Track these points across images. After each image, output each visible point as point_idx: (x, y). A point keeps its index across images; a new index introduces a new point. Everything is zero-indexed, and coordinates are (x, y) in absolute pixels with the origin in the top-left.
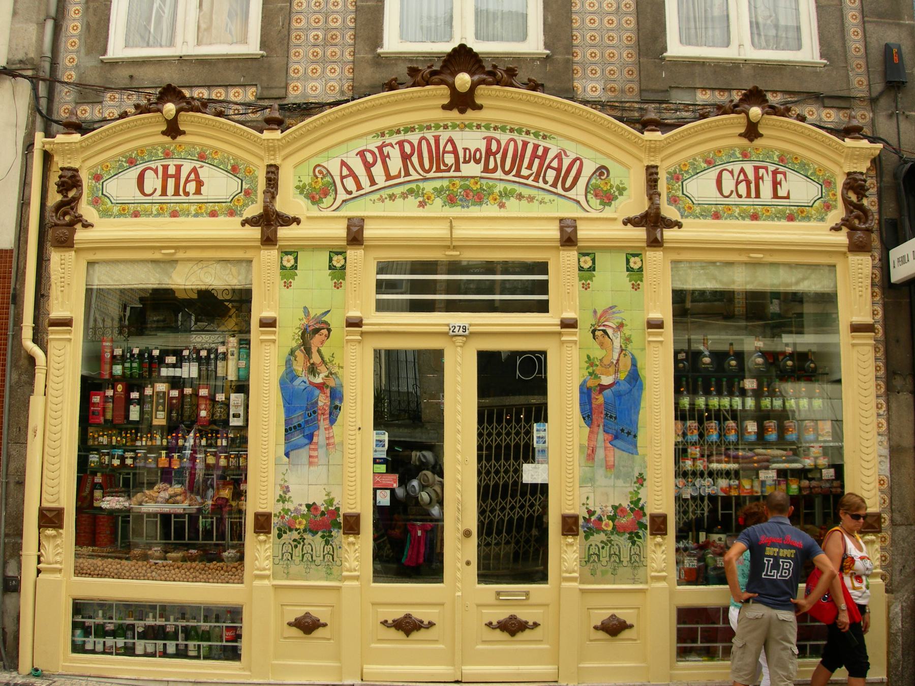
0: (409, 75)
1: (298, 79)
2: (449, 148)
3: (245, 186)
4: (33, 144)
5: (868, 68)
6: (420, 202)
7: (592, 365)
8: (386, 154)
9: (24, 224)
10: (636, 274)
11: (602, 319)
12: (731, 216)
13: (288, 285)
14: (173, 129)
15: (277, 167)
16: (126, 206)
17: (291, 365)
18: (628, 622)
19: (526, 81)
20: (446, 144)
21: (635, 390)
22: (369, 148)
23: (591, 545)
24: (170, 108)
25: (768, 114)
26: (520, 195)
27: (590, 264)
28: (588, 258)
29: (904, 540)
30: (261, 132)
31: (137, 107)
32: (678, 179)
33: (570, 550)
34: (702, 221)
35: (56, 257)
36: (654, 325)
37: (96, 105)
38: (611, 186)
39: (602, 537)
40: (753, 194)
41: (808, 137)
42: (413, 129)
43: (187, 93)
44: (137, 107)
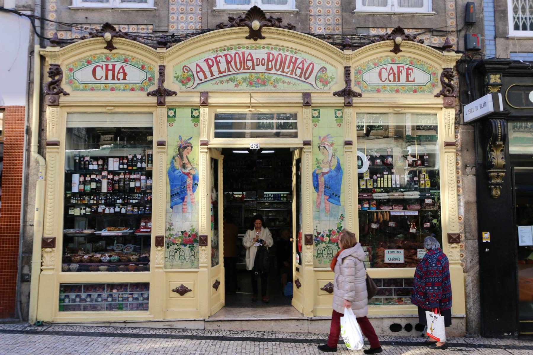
0: (229, 21)
1: (174, 22)
2: (249, 58)
3: (149, 76)
6: (235, 85)
8: (218, 61)
10: (339, 119)
11: (323, 142)
13: (171, 125)
15: (164, 66)
19: (286, 24)
20: (248, 56)
21: (339, 175)
22: (210, 58)
24: (108, 35)
25: (405, 40)
26: (284, 81)
27: (317, 114)
30: (156, 49)
32: (360, 73)
33: (308, 251)
36: (348, 143)
37: (68, 32)
38: (328, 77)
39: (324, 245)
40: (397, 80)
41: (425, 51)
42: (231, 49)
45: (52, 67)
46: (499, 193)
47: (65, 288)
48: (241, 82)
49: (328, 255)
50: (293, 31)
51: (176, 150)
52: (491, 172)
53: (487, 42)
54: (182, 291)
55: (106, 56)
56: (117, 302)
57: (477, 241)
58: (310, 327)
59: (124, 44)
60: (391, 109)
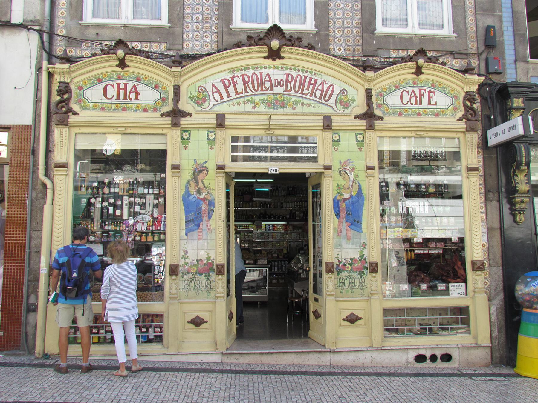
0: (247, 40)
1: (189, 40)
2: (267, 79)
4: (42, 68)
7: (339, 188)
8: (235, 81)
9: (38, 112)
10: (361, 144)
13: (186, 148)
16: (97, 104)
17: (188, 189)
20: (266, 76)
23: (340, 278)
24: (120, 53)
25: (427, 62)
26: (303, 103)
27: (338, 138)
30: (171, 68)
32: (381, 95)
35: (57, 132)
36: (370, 168)
40: (418, 103)
41: (447, 74)
42: (249, 69)
43: (129, 44)
44: (102, 50)
45: (62, 84)
48: (259, 104)
50: (313, 51)
51: (191, 174)
53: (507, 66)
54: (197, 322)
55: (117, 74)
57: (501, 268)
58: (332, 359)
59: (137, 62)
60: (413, 132)
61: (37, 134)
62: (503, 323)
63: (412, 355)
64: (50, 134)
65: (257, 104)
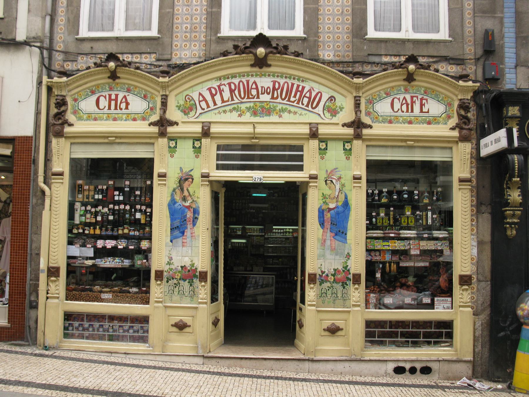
0: (234, 48)
2: (254, 86)
5: (475, 42)
6: (239, 114)
7: (325, 198)
8: (222, 89)
9: (38, 123)
10: (348, 152)
12: (398, 122)
13: (172, 156)
14: (113, 76)
16: (90, 115)
18: (341, 327)
19: (293, 51)
22: (214, 86)
25: (418, 68)
26: (290, 111)
27: (325, 146)
28: (324, 144)
29: (484, 290)
31: (95, 64)
34: (383, 124)
35: (54, 141)
36: (357, 178)
39: (328, 284)
40: (410, 111)
42: (235, 77)
44: (95, 64)
45: (59, 97)
46: (514, 232)
47: (69, 316)
49: (332, 294)
52: (507, 210)
54: (181, 326)
56: (118, 333)
57: (489, 283)
61: (37, 144)
62: (487, 339)
63: (391, 366)
64: (49, 144)
65: (243, 112)
